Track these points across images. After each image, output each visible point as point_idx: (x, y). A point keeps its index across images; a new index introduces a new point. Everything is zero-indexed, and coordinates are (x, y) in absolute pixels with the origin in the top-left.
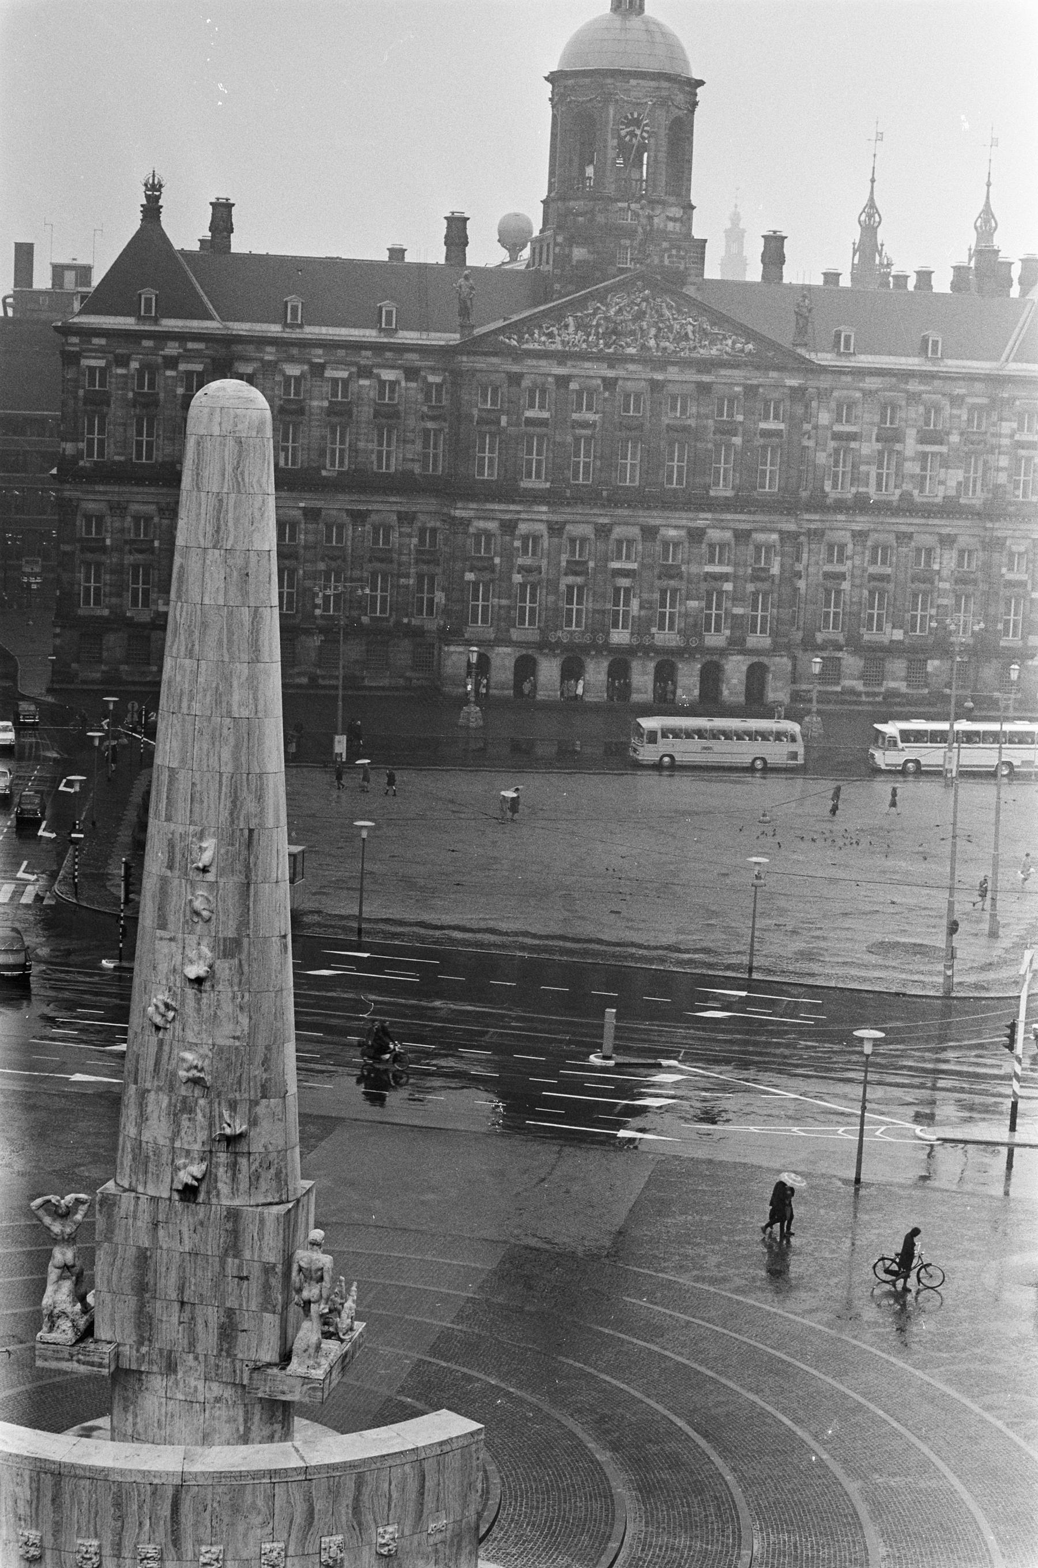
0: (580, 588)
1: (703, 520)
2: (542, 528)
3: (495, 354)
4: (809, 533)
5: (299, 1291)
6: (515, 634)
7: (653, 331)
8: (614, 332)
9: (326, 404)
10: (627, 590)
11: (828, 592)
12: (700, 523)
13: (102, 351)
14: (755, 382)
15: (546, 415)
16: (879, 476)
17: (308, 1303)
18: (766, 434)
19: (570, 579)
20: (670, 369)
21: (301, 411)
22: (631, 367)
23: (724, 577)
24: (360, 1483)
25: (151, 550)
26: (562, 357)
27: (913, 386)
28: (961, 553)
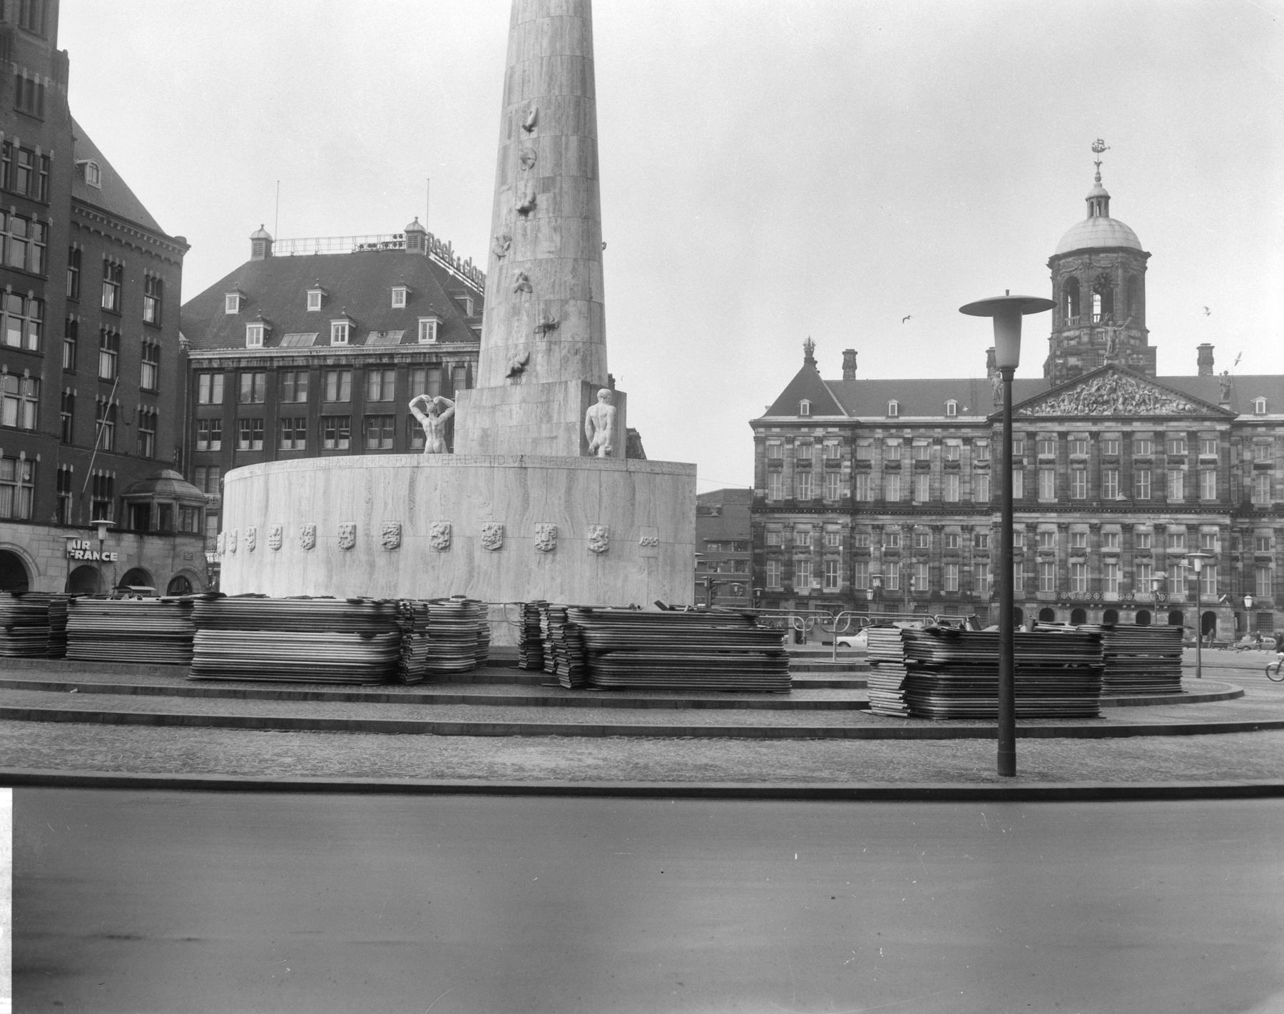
1: (1163, 519)
2: (1054, 528)
7: (1121, 400)
12: (1161, 521)
13: (778, 436)
15: (1052, 456)
18: (1204, 462)
21: (898, 467)
22: (1107, 424)
25: (809, 553)
26: (1060, 420)
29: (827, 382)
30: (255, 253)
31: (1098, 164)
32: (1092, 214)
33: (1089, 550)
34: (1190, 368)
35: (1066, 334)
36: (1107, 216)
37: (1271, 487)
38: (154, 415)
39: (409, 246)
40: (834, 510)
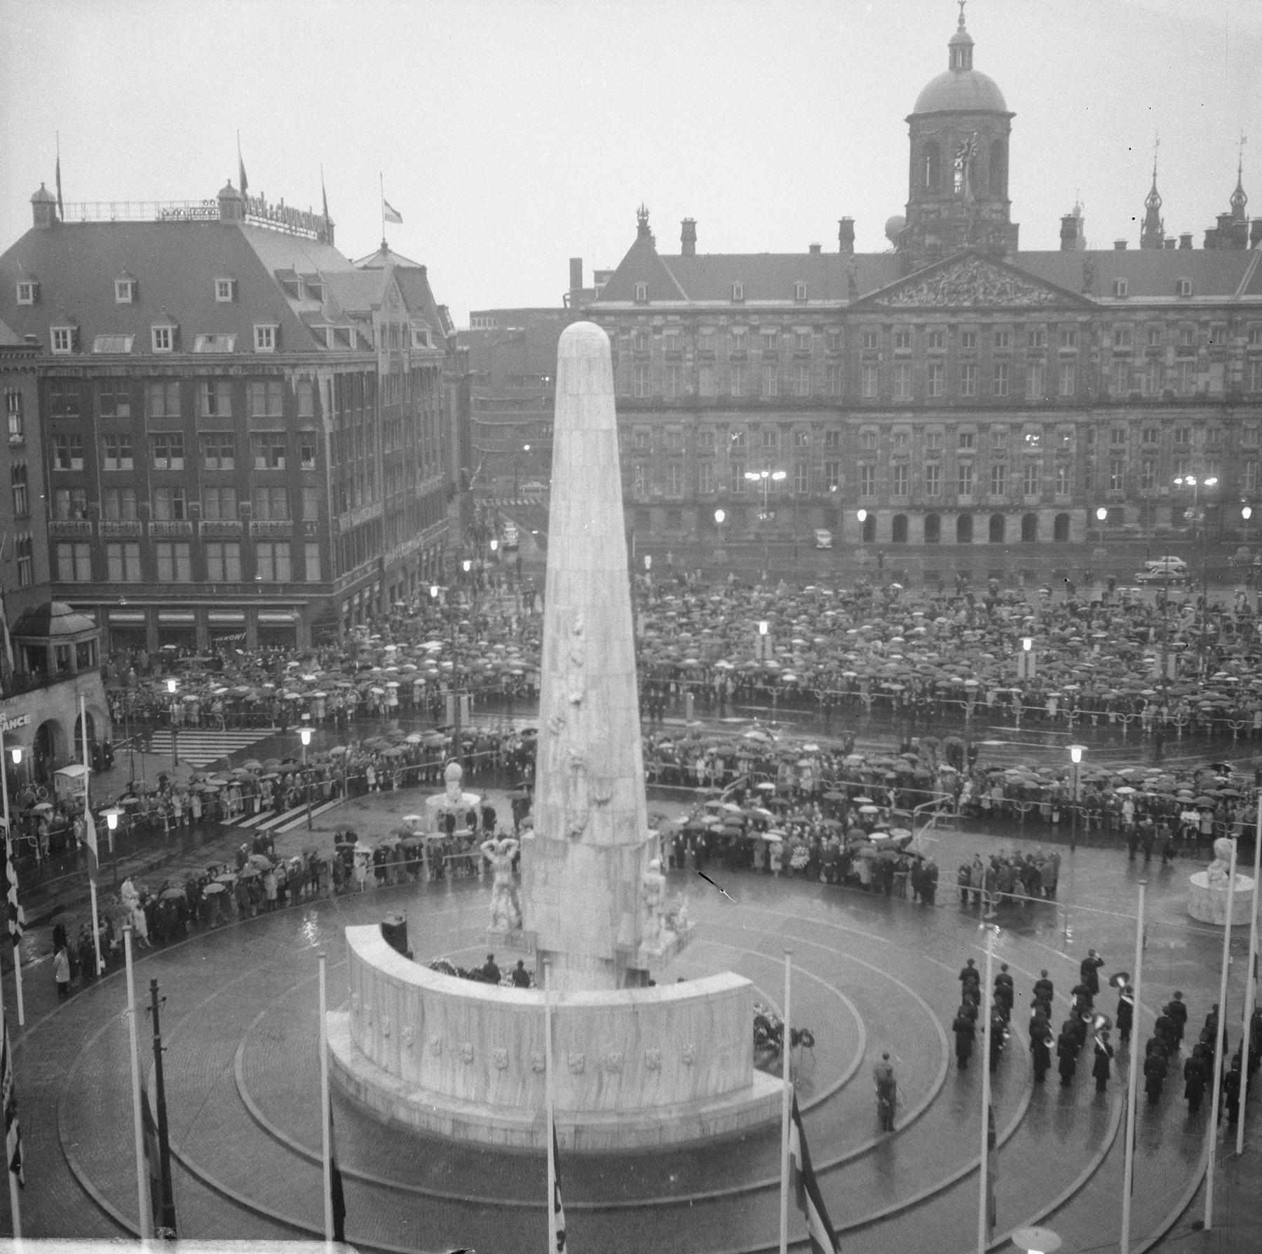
0: (937, 468)
1: (1021, 417)
2: (908, 429)
3: (873, 312)
4: (1098, 423)
5: (645, 899)
6: (893, 501)
8: (954, 292)
9: (761, 352)
10: (969, 468)
11: (1113, 462)
14: (1055, 320)
15: (908, 351)
16: (1148, 380)
17: (650, 907)
18: (1064, 355)
19: (930, 462)
20: (995, 315)
21: (744, 358)
22: (967, 315)
23: (1038, 456)
24: (670, 1015)
25: (649, 455)
27: (1172, 316)
28: (1210, 430)
29: (663, 256)
30: (37, 219)
31: (962, 4)
32: (953, 65)
33: (944, 451)
34: (1052, 242)
35: (924, 206)
36: (970, 67)
37: (1130, 375)
38: (29, 540)
39: (224, 215)
40: (675, 409)
